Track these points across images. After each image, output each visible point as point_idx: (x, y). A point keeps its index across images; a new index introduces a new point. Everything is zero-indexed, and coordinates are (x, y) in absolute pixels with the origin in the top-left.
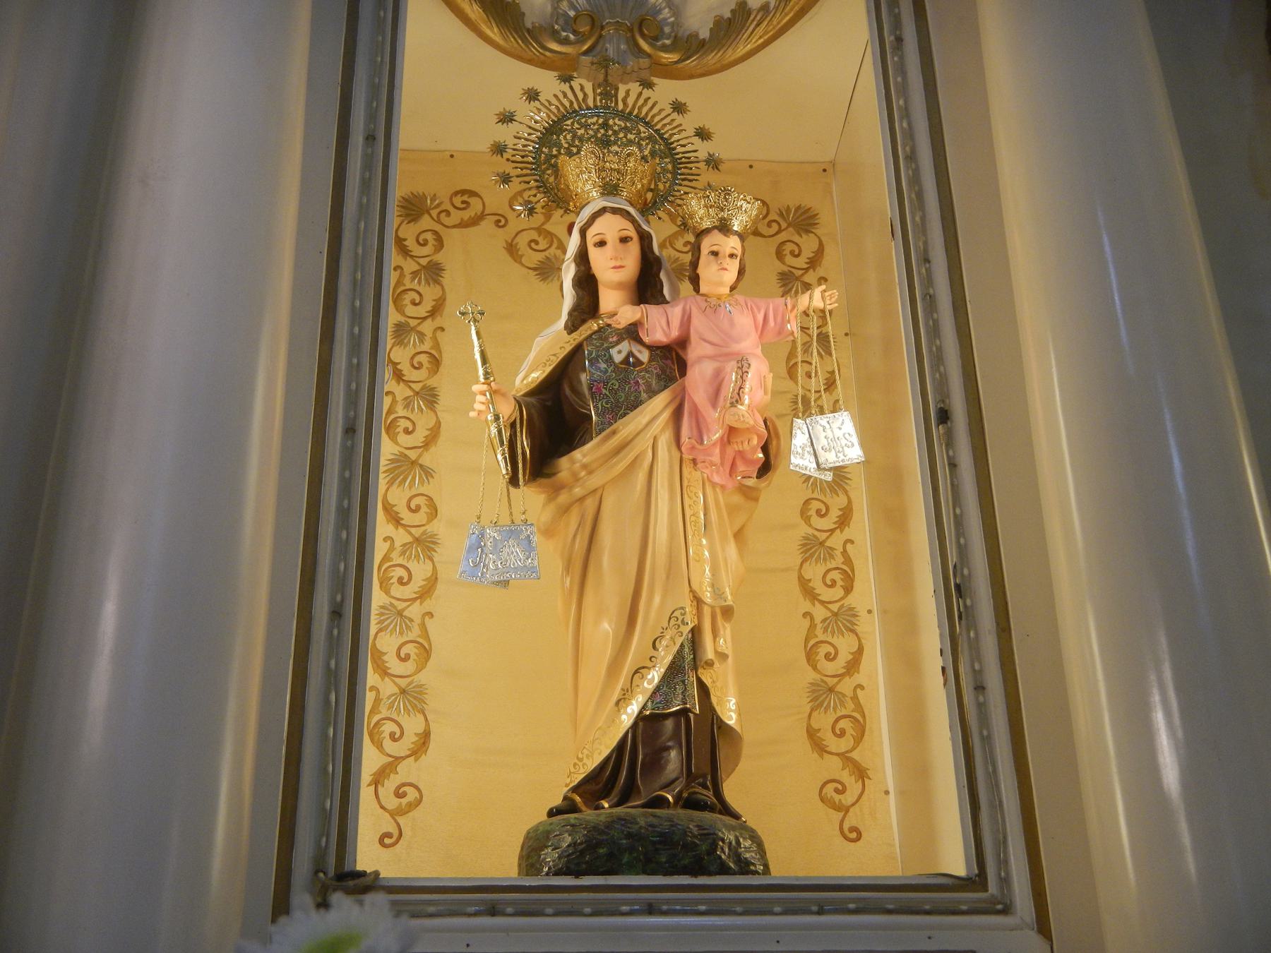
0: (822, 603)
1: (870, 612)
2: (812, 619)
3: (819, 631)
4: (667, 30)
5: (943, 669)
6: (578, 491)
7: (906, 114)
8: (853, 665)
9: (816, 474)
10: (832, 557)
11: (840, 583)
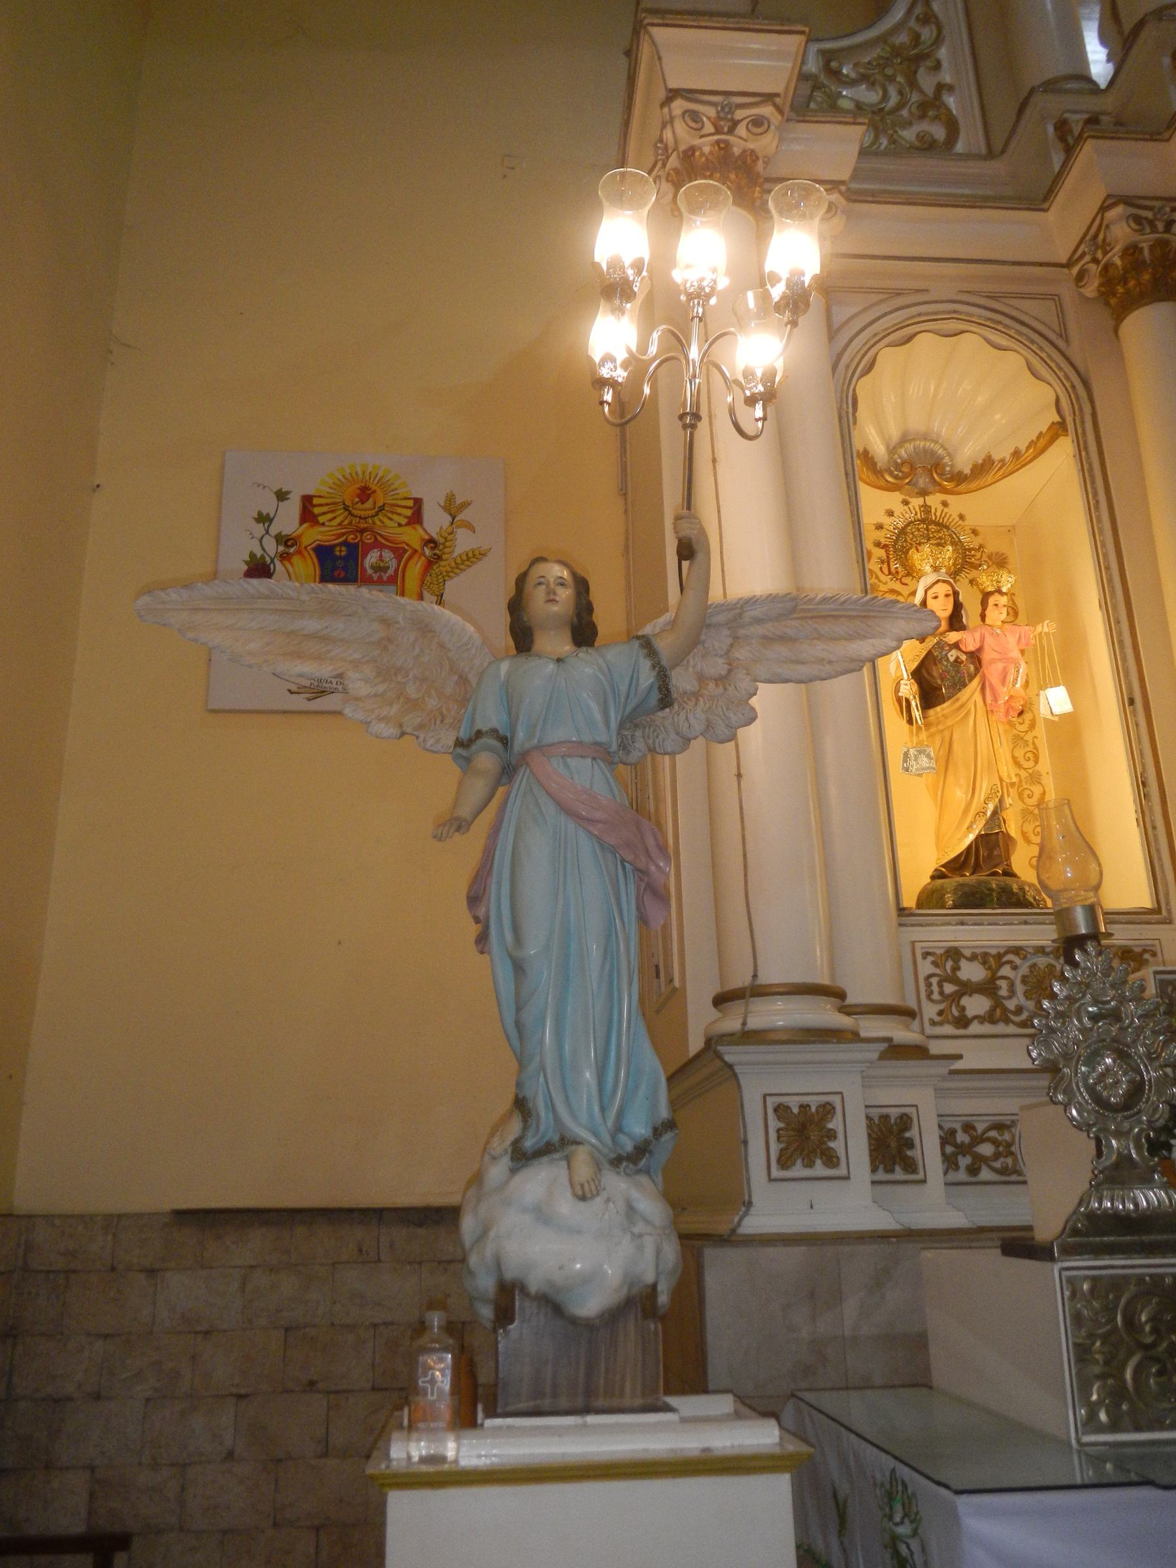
0: (1025, 769)
1: (1047, 773)
2: (1020, 778)
3: (1024, 784)
4: (948, 469)
5: (1137, 819)
6: (941, 727)
7: (1103, 545)
9: (1050, 717)
10: (1027, 745)
11: (1032, 758)
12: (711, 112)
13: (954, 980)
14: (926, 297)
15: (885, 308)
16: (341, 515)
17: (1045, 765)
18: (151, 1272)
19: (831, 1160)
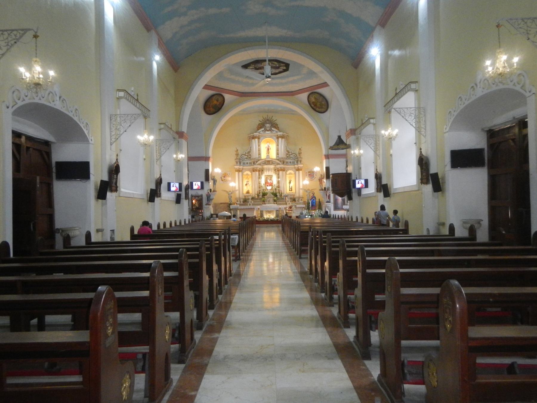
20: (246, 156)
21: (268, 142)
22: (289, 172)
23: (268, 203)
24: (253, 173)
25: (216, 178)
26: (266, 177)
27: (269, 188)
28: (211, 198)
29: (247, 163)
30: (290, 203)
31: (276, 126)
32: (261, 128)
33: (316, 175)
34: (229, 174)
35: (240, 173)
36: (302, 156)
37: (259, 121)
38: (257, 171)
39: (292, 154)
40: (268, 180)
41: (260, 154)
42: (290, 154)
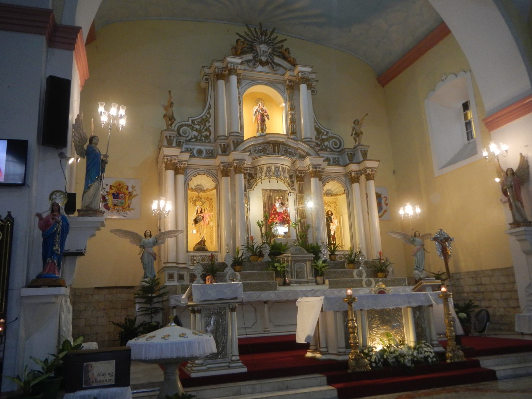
8: (213, 234)
12: (169, 158)
13: (193, 259)
14: (199, 170)
15: (194, 171)
16: (116, 188)
17: (214, 228)
18: (92, 295)
19: (173, 278)
20: (196, 130)
21: (258, 99)
22: (325, 188)
23: (296, 283)
24: (224, 179)
25: (101, 148)
26: (267, 195)
27: (281, 230)
28: (70, 245)
29: (200, 152)
30: (372, 280)
31: (287, 54)
32: (243, 53)
33: (387, 204)
34: (133, 187)
35: (181, 178)
36: (364, 140)
37: (237, 34)
38: (240, 172)
39: (328, 140)
40: (277, 205)
41: (242, 128)
42: (324, 137)
